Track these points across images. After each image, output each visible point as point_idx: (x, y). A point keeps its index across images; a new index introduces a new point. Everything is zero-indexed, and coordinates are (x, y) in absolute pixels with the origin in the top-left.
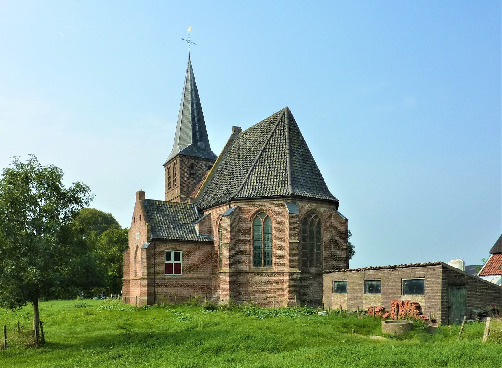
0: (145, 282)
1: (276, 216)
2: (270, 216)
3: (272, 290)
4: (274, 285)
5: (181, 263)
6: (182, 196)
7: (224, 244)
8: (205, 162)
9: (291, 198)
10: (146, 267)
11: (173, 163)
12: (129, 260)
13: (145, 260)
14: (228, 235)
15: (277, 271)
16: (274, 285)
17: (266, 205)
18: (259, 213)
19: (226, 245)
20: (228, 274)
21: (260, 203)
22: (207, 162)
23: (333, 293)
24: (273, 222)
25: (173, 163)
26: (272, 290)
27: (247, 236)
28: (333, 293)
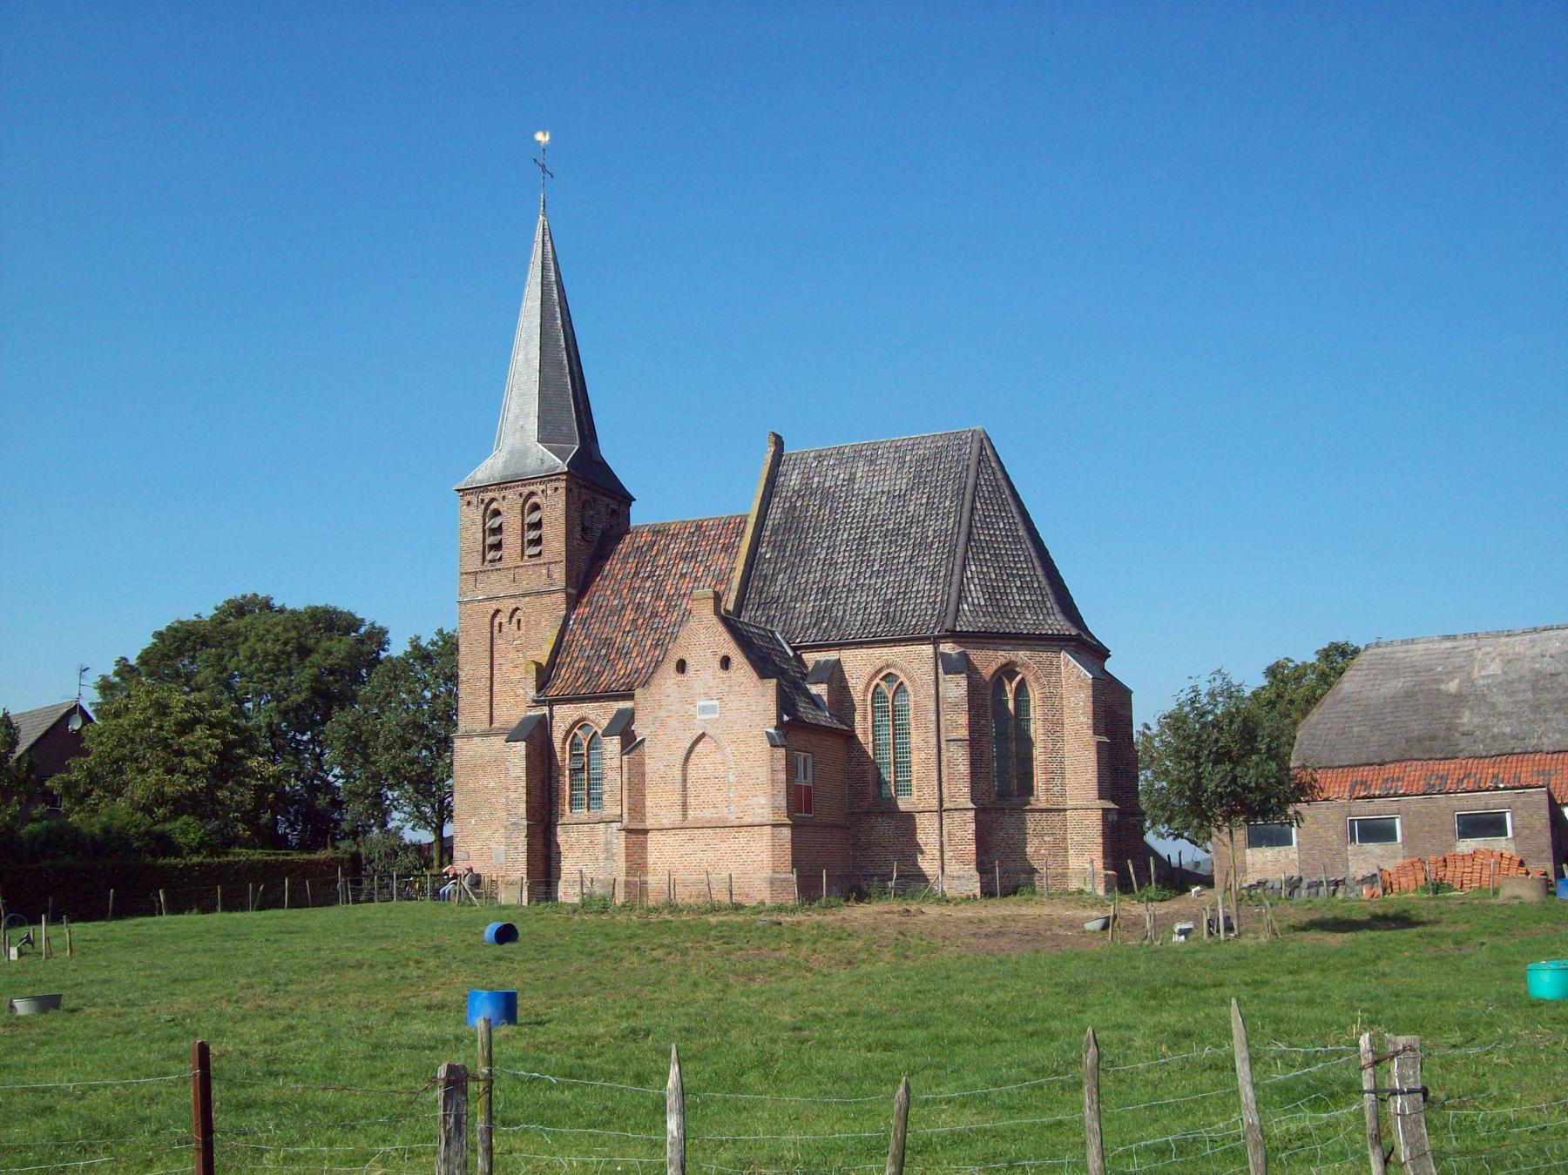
0: (786, 833)
1: (1044, 681)
2: (1030, 679)
3: (1042, 852)
4: (1046, 839)
5: (811, 784)
6: (570, 590)
7: (954, 740)
9: (1073, 643)
10: (783, 793)
11: (526, 491)
12: (644, 775)
13: (782, 776)
14: (963, 719)
15: (1049, 807)
16: (1046, 839)
17: (1022, 655)
18: (1008, 671)
19: (960, 743)
20: (971, 814)
22: (611, 501)
23: (1353, 839)
24: (1035, 695)
26: (1042, 852)
27: (983, 722)
28: (1353, 839)
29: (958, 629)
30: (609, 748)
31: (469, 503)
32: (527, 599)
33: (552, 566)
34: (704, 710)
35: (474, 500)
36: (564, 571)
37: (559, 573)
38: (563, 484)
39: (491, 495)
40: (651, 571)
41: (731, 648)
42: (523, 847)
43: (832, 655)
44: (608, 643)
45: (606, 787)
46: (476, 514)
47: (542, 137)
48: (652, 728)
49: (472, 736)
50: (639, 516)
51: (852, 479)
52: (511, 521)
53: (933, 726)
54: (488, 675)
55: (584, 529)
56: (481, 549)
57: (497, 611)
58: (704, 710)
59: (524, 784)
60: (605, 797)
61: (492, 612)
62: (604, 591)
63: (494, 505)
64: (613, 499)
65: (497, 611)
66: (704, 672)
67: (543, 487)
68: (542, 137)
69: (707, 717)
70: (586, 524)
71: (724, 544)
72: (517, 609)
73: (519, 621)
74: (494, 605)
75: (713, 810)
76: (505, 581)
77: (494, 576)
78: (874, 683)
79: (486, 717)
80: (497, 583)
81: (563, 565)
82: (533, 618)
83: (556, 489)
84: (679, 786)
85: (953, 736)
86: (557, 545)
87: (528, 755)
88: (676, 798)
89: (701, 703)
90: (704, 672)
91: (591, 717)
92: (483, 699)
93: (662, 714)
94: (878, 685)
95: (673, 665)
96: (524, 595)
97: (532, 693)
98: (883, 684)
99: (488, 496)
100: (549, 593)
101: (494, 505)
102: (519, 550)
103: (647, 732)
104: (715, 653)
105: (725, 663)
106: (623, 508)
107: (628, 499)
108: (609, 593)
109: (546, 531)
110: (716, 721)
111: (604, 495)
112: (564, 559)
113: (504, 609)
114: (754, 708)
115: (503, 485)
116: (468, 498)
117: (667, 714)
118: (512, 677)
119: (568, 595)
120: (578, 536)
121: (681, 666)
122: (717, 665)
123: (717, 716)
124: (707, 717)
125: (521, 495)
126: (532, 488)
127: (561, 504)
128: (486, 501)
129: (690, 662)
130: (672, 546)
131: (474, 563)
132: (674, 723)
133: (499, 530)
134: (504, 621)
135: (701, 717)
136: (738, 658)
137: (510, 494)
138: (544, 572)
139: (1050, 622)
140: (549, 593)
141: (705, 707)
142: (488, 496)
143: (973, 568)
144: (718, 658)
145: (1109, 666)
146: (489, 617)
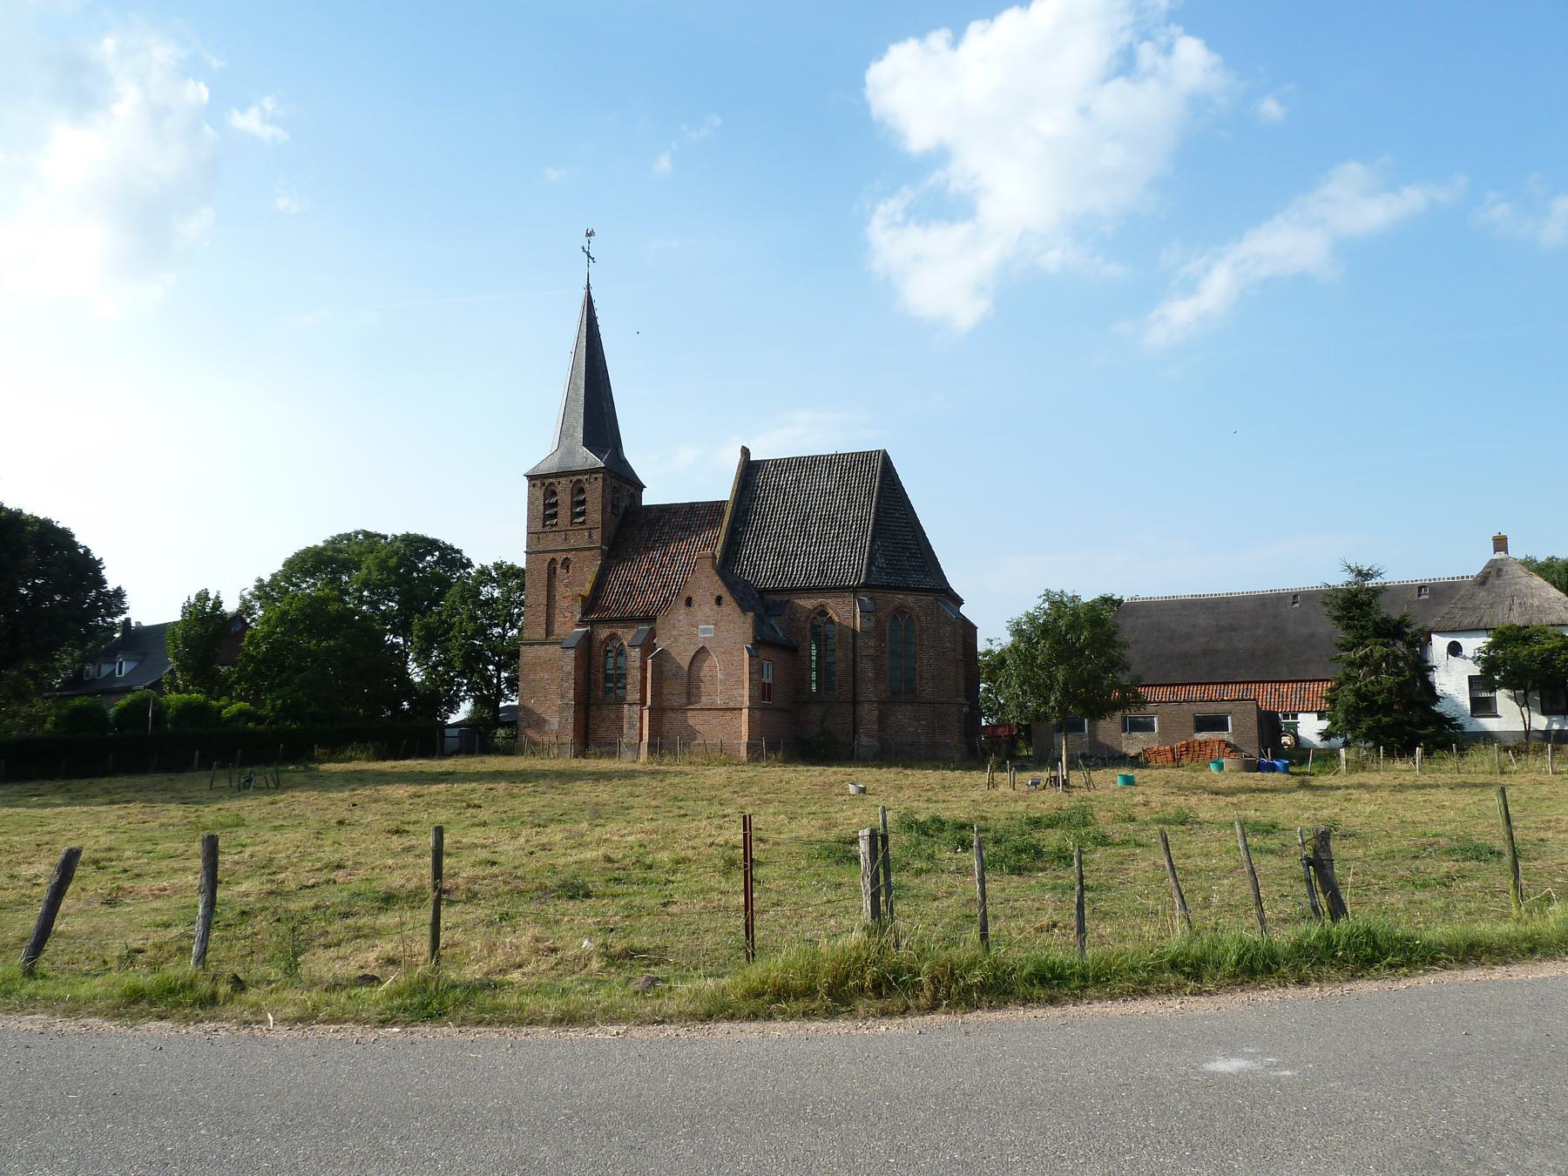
8: (628, 487)
11: (575, 479)
16: (922, 722)
21: (901, 596)
25: (575, 479)
29: (869, 583)
30: (633, 654)
31: (534, 485)
33: (592, 531)
34: (704, 631)
37: (597, 535)
38: (601, 475)
40: (659, 537)
41: (723, 591)
42: (571, 720)
43: (785, 598)
44: (630, 583)
45: (629, 680)
46: (540, 493)
48: (668, 642)
49: (533, 644)
50: (648, 499)
51: (798, 480)
52: (564, 497)
53: (851, 646)
55: (613, 505)
56: (542, 517)
57: (553, 560)
58: (704, 631)
59: (573, 677)
60: (628, 687)
64: (632, 486)
66: (705, 608)
69: (707, 636)
70: (615, 502)
71: (709, 520)
74: (551, 555)
75: (709, 698)
77: (551, 535)
78: (812, 616)
80: (554, 541)
83: (596, 479)
84: (685, 680)
85: (865, 653)
86: (597, 516)
87: (576, 658)
89: (702, 627)
90: (705, 608)
93: (675, 633)
94: (815, 618)
95: (684, 601)
96: (572, 550)
97: (578, 616)
98: (817, 617)
99: (547, 482)
100: (590, 549)
103: (664, 645)
104: (712, 594)
105: (719, 600)
106: (638, 492)
107: (641, 487)
108: (630, 549)
109: (588, 507)
110: (710, 639)
111: (627, 483)
112: (600, 526)
113: (558, 559)
115: (557, 475)
116: (534, 482)
117: (677, 633)
119: (603, 550)
120: (609, 510)
121: (689, 602)
122: (714, 602)
125: (571, 481)
127: (600, 490)
130: (673, 520)
131: (540, 528)
133: (555, 505)
136: (727, 597)
137: (563, 481)
139: (928, 580)
140: (590, 549)
141: (705, 629)
143: (879, 543)
144: (714, 597)
145: (962, 610)
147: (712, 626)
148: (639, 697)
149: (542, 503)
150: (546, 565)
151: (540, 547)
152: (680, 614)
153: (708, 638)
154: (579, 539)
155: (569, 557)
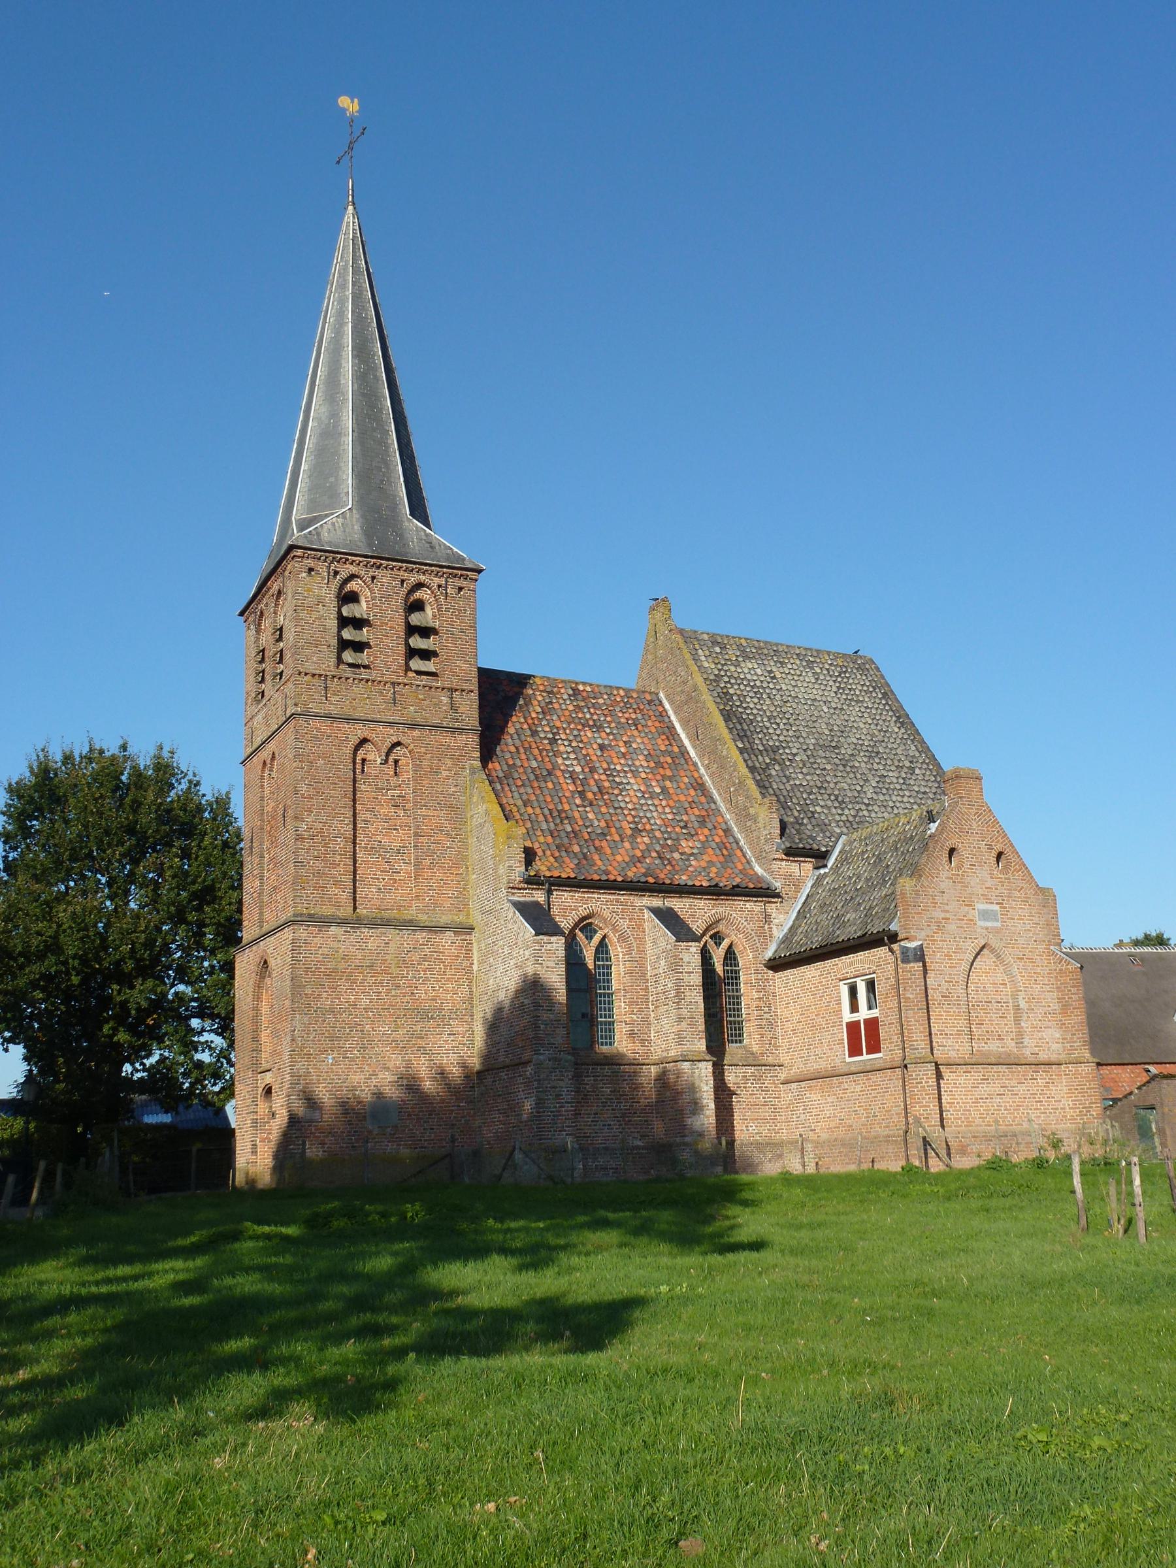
11: (413, 579)
30: (686, 958)
32: (416, 733)
34: (985, 915)
35: (322, 568)
36: (476, 705)
39: (353, 569)
47: (349, 105)
54: (349, 834)
57: (364, 741)
58: (985, 915)
61: (355, 740)
62: (508, 744)
63: (353, 586)
65: (364, 741)
67: (437, 581)
68: (349, 105)
69: (989, 924)
72: (398, 744)
73: (396, 762)
74: (360, 732)
75: (998, 1043)
76: (379, 700)
77: (359, 689)
79: (346, 895)
81: (475, 696)
82: (425, 762)
88: (962, 1023)
91: (606, 914)
92: (341, 869)
96: (414, 726)
101: (353, 586)
102: (401, 660)
110: (997, 931)
114: (1036, 920)
117: (943, 915)
118: (385, 842)
122: (993, 860)
123: (998, 924)
124: (989, 924)
125: (403, 581)
126: (422, 578)
128: (343, 575)
129: (964, 852)
132: (952, 927)
134: (369, 757)
135: (982, 923)
138: (445, 700)
142: (346, 570)
144: (994, 854)
146: (351, 746)
147: (996, 907)
148: (704, 1048)
149: (334, 615)
150: (348, 751)
151: (333, 710)
152: (942, 875)
153: (992, 928)
154: (437, 707)
155: (404, 740)
